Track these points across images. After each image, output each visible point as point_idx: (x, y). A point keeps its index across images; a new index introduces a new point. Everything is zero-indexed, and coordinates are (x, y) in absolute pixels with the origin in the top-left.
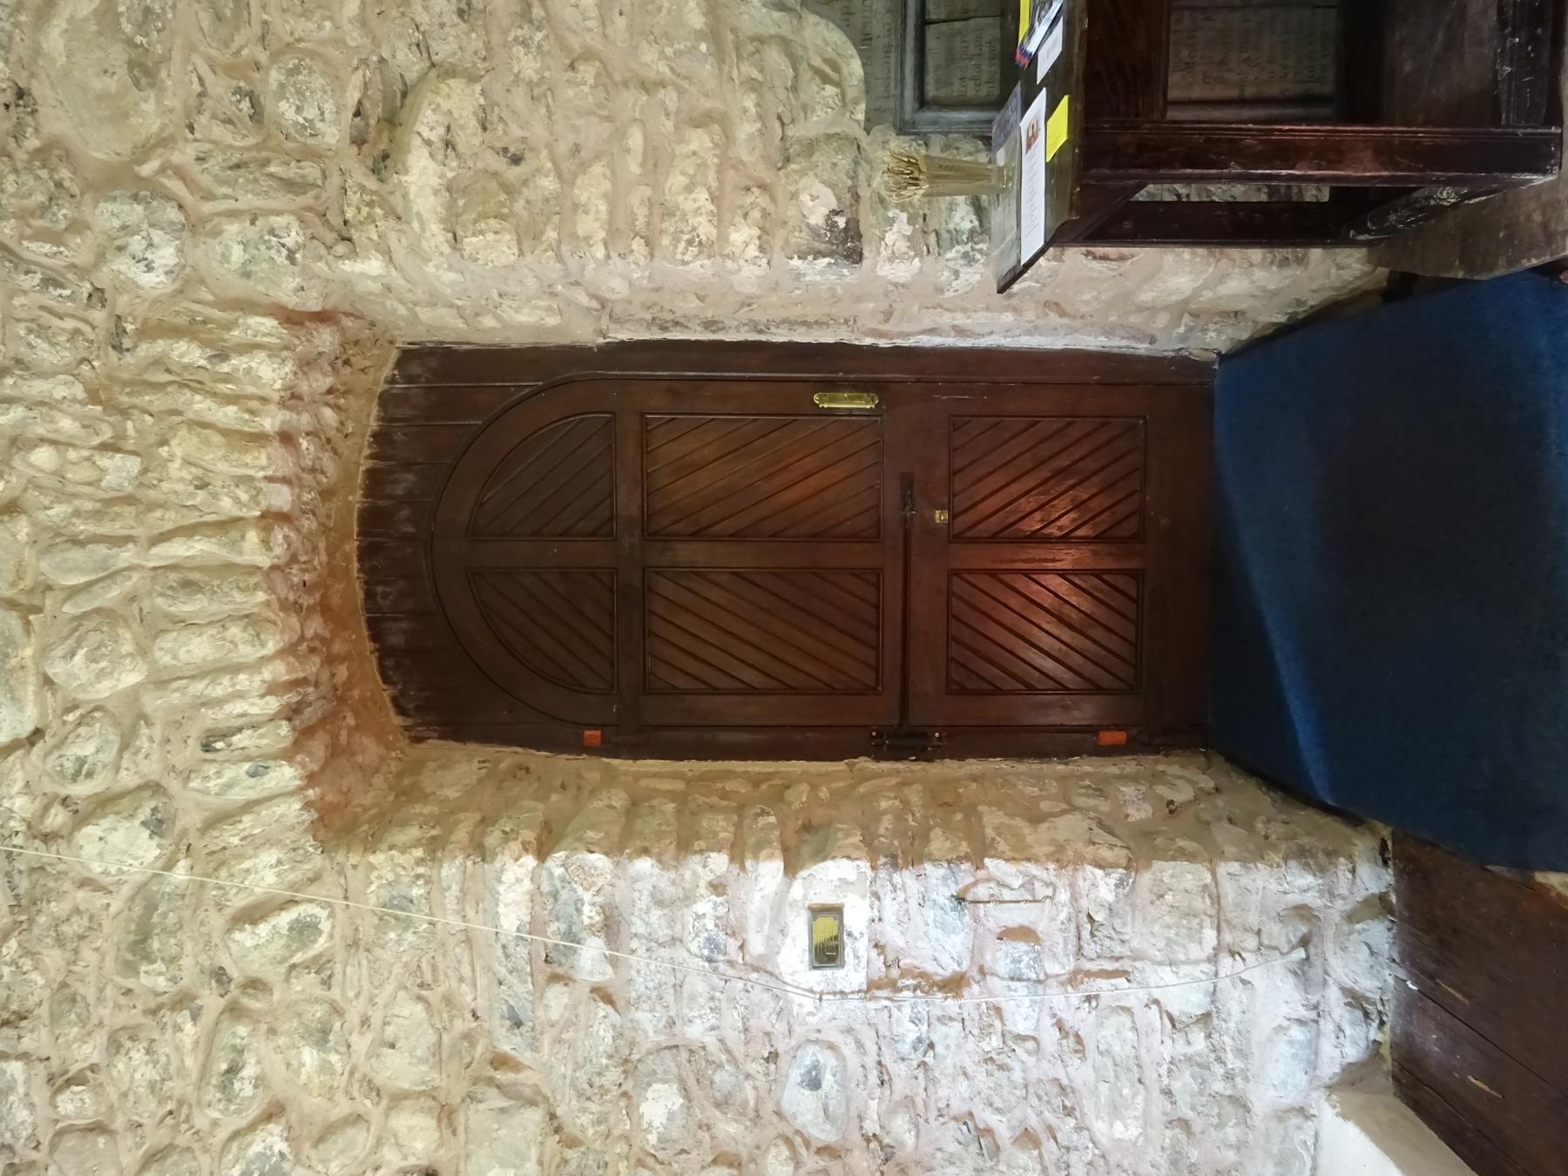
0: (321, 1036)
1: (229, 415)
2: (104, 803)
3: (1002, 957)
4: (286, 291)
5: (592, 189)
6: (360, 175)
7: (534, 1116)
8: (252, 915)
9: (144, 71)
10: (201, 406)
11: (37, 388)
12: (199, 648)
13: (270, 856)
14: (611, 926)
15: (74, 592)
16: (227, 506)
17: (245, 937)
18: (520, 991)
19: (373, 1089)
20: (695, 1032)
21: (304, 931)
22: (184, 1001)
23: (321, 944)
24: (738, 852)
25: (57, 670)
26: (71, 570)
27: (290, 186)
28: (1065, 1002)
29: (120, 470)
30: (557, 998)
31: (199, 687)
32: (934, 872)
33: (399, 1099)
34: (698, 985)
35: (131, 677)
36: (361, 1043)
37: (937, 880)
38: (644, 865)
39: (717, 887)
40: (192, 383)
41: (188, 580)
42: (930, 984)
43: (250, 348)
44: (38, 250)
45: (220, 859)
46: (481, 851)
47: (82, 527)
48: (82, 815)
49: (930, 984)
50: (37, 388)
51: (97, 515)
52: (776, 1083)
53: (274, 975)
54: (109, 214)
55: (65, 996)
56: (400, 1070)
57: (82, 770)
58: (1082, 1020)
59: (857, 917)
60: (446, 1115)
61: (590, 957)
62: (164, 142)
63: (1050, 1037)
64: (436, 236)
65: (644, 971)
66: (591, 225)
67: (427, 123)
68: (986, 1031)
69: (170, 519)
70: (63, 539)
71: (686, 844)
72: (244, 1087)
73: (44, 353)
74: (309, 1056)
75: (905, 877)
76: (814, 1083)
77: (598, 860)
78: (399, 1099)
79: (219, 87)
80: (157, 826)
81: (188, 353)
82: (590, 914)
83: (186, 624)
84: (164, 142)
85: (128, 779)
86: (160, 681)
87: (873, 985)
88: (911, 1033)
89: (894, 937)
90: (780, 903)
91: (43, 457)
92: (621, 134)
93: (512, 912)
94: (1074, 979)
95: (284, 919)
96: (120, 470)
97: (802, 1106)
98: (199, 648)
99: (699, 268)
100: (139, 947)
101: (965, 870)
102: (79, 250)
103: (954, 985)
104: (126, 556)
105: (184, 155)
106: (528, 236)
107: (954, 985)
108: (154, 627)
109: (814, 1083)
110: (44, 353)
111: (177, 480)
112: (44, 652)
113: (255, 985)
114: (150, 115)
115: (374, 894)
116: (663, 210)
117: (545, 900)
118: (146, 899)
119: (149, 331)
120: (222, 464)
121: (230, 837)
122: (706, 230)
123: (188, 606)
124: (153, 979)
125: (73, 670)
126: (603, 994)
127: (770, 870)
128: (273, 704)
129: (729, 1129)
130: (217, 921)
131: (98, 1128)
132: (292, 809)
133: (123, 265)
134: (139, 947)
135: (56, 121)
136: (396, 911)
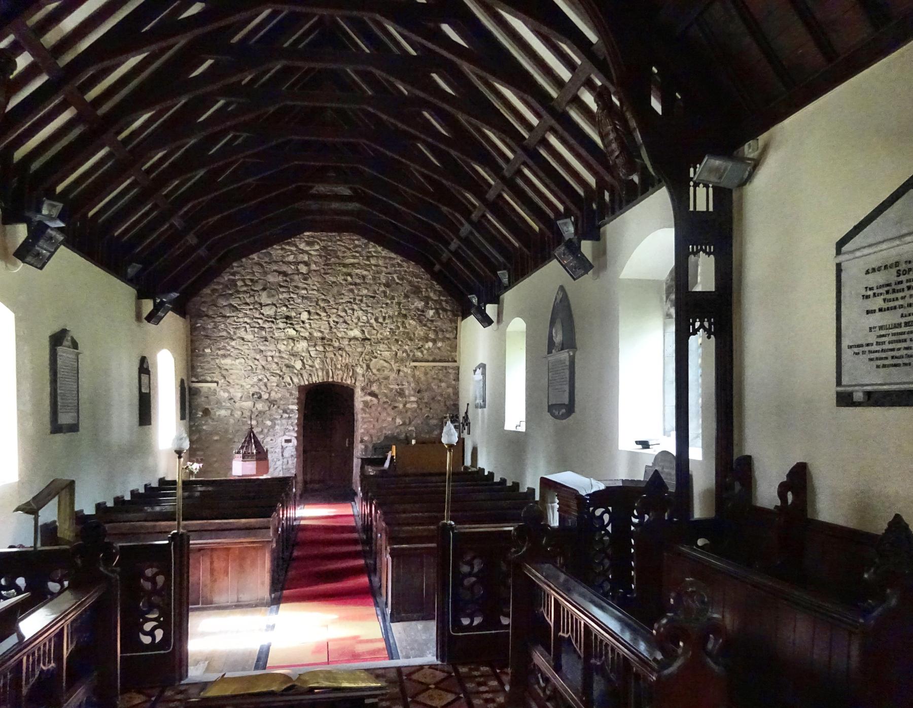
0: (277, 386)
1: (345, 378)
2: (303, 363)
3: (285, 460)
4: (357, 384)
5: (368, 415)
6: (369, 391)
7: (268, 409)
8: (291, 379)
9: (378, 370)
10: (345, 375)
11: (347, 358)
12: (320, 374)
13: (298, 381)
14: (289, 418)
15: (326, 361)
16: (335, 377)
17: (289, 378)
18: (282, 407)
19: (271, 390)
20: (277, 427)
21: (289, 384)
22: (281, 371)
23: (288, 386)
24: (297, 432)
25: (318, 359)
26: (328, 360)
27: (367, 384)
28: (280, 468)
29: (339, 366)
30: (281, 411)
31: (316, 374)
32: (295, 453)
33: (269, 394)
34: (282, 427)
35: (317, 366)
36: (276, 390)
37: (294, 453)
38: (296, 421)
39: (294, 429)
40: (348, 374)
41: (327, 373)
42: (282, 452)
43: (351, 380)
44: (361, 359)
45: (297, 376)
46: (297, 404)
47: (333, 362)
48: (302, 360)
49: (282, 452)
50: (347, 358)
51: (334, 364)
52: (271, 436)
53: (284, 380)
54: (365, 366)
55: (282, 357)
56: (273, 394)
57: (307, 361)
58: (278, 470)
59: (290, 444)
60: (267, 399)
61: (286, 415)
62: (372, 372)
63: (276, 466)
64: (363, 399)
65: (284, 421)
66: (364, 415)
67: (374, 399)
68: (277, 459)
69: (334, 370)
70: (332, 360)
71: (298, 425)
72: (272, 377)
73: (351, 359)
74: (275, 384)
75: (294, 449)
76: (271, 440)
77: (297, 416)
78: (269, 394)
79: (376, 378)
80: (301, 369)
81: (351, 374)
82: (291, 415)
83: (323, 373)
84: (372, 372)
85: (306, 366)
86: (317, 370)
87: (282, 446)
88: (277, 450)
89: (288, 448)
90: (292, 436)
91: (340, 359)
92: (372, 418)
93: (291, 407)
94: (283, 468)
95: (291, 382)
96: (339, 366)
97: (268, 439)
98: (320, 374)
99: (360, 426)
100: (288, 366)
101: (295, 456)
102: (361, 363)
103: (282, 455)
104: (330, 367)
105: (370, 373)
106: (362, 409)
107: (282, 455)
108: (322, 370)
109: (271, 440)
110: (351, 359)
111: (338, 372)
112: (320, 358)
113: (283, 378)
114: (374, 371)
115: (293, 392)
116: (365, 423)
117: (292, 411)
118: (293, 367)
119: (353, 370)
120: (340, 377)
121: (300, 377)
122: (363, 427)
123: (324, 372)
124: (284, 369)
125: (318, 361)
126: (282, 416)
127: (295, 435)
128: (314, 382)
129: (266, 431)
130: (291, 375)
131: (267, 361)
132: (302, 384)
133: (359, 368)
134: (288, 366)
135: (374, 360)
136: (291, 394)
